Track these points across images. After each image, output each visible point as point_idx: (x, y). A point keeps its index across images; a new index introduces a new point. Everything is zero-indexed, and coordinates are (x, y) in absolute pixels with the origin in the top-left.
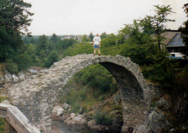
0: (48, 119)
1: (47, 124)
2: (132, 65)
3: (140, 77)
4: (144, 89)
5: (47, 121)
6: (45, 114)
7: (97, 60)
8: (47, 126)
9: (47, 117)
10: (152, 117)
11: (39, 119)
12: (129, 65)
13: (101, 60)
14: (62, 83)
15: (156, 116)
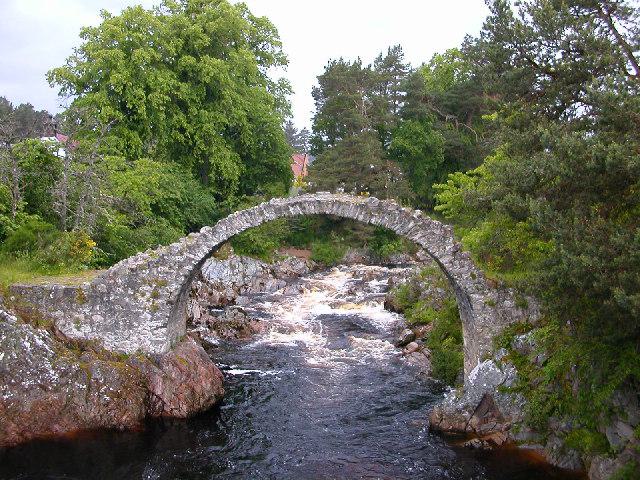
0: (157, 328)
1: (153, 338)
2: (426, 226)
3: (457, 262)
4: (475, 296)
5: (156, 332)
6: (149, 316)
7: (291, 209)
8: (157, 343)
9: (154, 324)
10: (479, 375)
11: (136, 324)
12: (412, 224)
13: (304, 208)
14: (192, 256)
15: (491, 374)
